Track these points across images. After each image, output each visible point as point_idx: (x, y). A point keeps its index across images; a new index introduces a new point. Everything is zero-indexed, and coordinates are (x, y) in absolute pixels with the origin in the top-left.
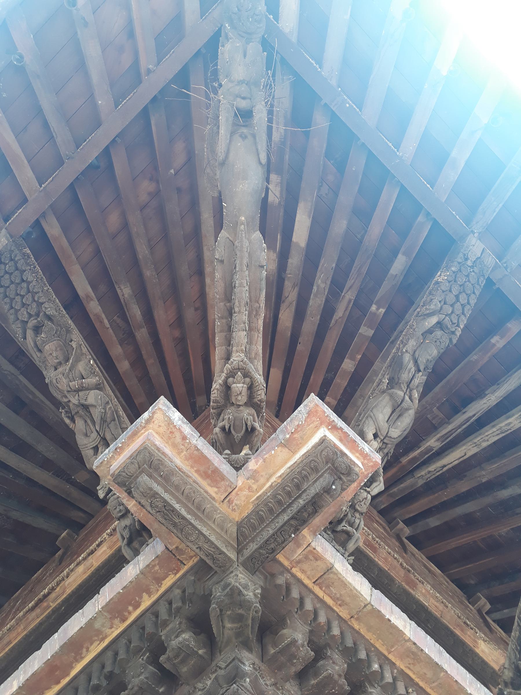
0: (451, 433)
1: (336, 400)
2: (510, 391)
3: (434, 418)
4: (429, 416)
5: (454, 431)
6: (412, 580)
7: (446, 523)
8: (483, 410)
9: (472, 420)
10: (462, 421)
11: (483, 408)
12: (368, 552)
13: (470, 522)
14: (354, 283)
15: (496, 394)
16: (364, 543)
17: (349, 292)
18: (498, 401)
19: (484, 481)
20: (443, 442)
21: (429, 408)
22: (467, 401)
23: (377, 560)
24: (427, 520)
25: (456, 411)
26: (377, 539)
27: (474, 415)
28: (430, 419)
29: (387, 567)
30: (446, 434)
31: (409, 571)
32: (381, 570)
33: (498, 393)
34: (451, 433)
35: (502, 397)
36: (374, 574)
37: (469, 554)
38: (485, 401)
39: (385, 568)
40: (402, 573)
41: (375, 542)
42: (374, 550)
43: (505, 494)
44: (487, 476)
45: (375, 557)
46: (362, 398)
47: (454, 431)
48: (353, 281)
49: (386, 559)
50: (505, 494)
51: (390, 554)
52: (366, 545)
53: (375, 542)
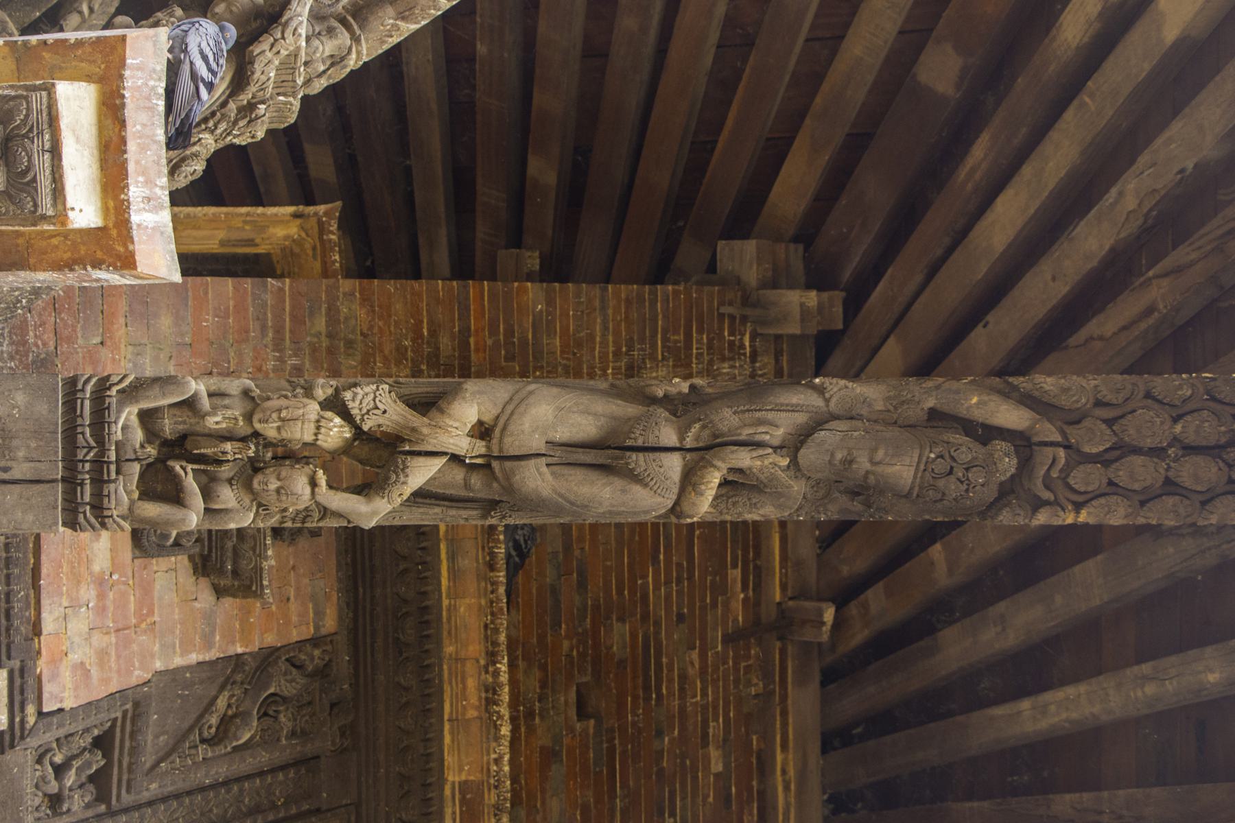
12: (448, 811)
14: (1192, 264)
16: (464, 786)
17: (1165, 282)
46: (999, 629)
48: (1194, 256)
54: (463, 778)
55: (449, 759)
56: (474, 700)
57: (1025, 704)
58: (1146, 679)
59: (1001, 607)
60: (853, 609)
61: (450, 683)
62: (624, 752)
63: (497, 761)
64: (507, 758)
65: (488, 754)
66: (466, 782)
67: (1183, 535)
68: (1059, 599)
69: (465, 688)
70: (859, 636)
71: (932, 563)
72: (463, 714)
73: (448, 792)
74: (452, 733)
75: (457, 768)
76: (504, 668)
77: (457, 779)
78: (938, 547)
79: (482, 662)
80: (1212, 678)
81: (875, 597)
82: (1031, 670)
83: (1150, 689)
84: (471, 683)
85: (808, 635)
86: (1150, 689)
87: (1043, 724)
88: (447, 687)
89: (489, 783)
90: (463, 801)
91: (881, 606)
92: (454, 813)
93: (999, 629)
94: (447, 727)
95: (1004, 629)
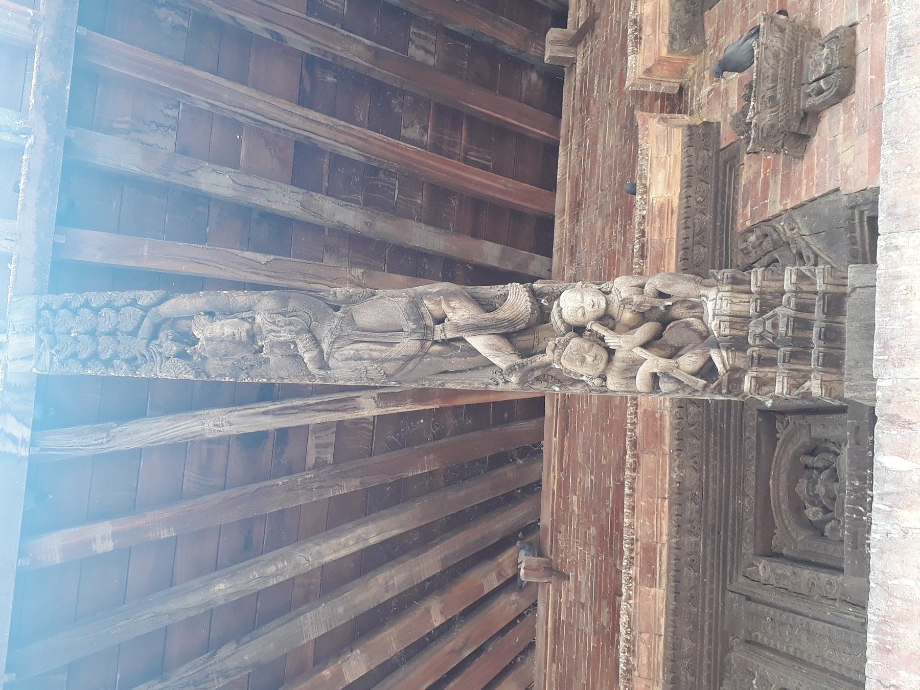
0: (327, 407)
1: (428, 611)
2: (170, 417)
3: (326, 446)
4: (329, 457)
5: (320, 407)
6: (646, 427)
7: (475, 234)
8: (245, 412)
9: (278, 405)
10: (292, 417)
11: (241, 416)
12: (664, 567)
13: (440, 203)
15: (199, 428)
16: (652, 584)
18: (206, 412)
19: (359, 271)
20: (352, 399)
21: (316, 485)
22: (252, 441)
23: (665, 538)
24: (496, 264)
25: (283, 434)
26: (626, 553)
27: (265, 413)
28: (331, 450)
29: (663, 506)
30: (336, 410)
31: (634, 444)
32: (679, 527)
33: (195, 429)
34: (327, 407)
35: (194, 416)
36: (697, 544)
37: (493, 138)
38: (227, 430)
39: (666, 509)
40: (648, 459)
41: (633, 555)
42: (650, 552)
43: (350, 217)
44: (348, 276)
45: (663, 545)
46: (390, 583)
47: (320, 407)
49: (650, 513)
50: (350, 217)
51: (633, 508)
52: (653, 579)
53: (633, 555)
54: (653, 590)
55: (661, 605)
56: (643, 647)
57: (373, 541)
58: (275, 575)
59: (387, 596)
60: (510, 573)
61: (658, 664)
62: (607, 536)
63: (630, 598)
64: (623, 597)
65: (635, 604)
66: (651, 587)
67: (236, 668)
68: (341, 610)
69: (649, 658)
70: (505, 558)
71: (442, 613)
72: (650, 638)
73: (664, 581)
74: (660, 626)
75: (657, 597)
76: (621, 665)
77: (657, 590)
78: (436, 625)
79: (636, 673)
80: (222, 586)
81: (491, 582)
82: (369, 561)
83: (272, 569)
84: (645, 661)
85: (535, 561)
86: (272, 569)
87: (359, 531)
88: (661, 660)
89: (636, 582)
90: (653, 573)
91: (487, 578)
92: (660, 566)
93: (390, 583)
94: (663, 631)
95: (387, 583)
